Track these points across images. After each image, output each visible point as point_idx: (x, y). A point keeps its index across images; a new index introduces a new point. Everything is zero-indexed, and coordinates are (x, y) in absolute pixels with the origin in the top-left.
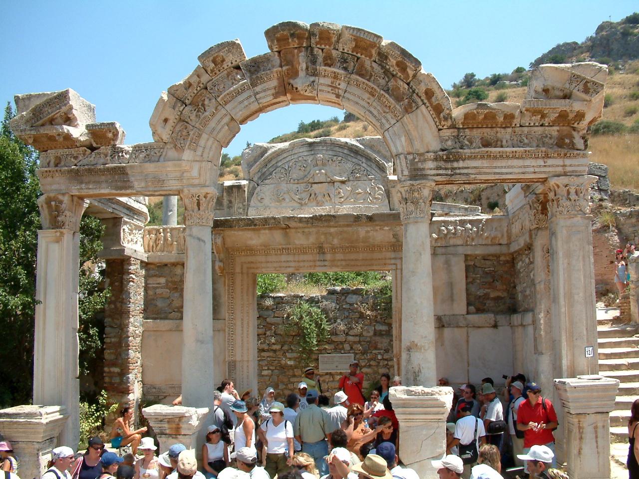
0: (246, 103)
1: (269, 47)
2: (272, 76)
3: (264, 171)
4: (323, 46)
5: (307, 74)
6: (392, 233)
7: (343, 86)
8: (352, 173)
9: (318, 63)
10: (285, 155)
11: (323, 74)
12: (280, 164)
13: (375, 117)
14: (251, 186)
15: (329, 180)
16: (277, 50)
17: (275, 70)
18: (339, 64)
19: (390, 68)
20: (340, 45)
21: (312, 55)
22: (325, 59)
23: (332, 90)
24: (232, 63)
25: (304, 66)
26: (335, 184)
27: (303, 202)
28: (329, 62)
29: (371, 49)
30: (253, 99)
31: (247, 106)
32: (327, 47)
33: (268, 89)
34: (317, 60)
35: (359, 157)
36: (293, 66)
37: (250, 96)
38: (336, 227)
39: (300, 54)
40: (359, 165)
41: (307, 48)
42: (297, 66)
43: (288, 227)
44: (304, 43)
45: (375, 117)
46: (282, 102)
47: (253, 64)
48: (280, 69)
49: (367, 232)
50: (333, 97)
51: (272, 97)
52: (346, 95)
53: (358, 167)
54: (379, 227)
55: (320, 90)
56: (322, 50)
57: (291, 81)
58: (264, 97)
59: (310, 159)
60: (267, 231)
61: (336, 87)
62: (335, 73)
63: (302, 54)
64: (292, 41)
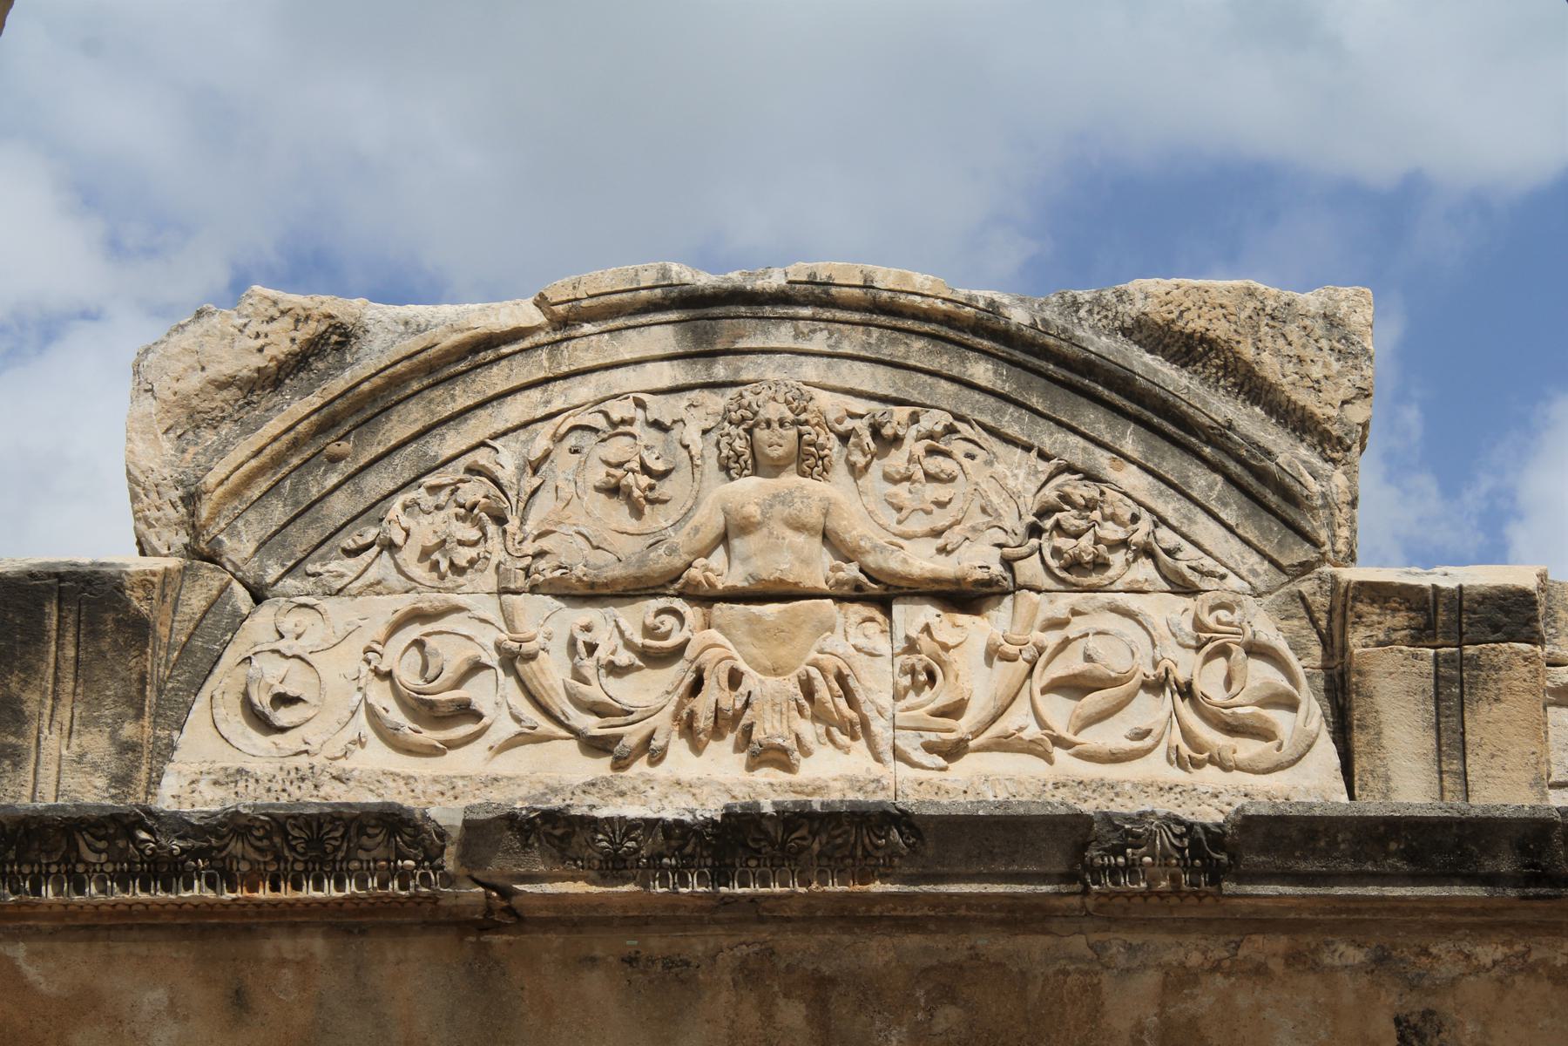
3: (315, 493)
6: (1390, 1001)
8: (1035, 531)
10: (497, 379)
12: (451, 442)
14: (195, 600)
15: (851, 571)
26: (898, 609)
27: (632, 736)
35: (1093, 419)
38: (915, 925)
40: (1091, 477)
43: (505, 914)
49: (1180, 980)
53: (1081, 491)
54: (1281, 943)
59: (697, 417)
60: (318, 945)
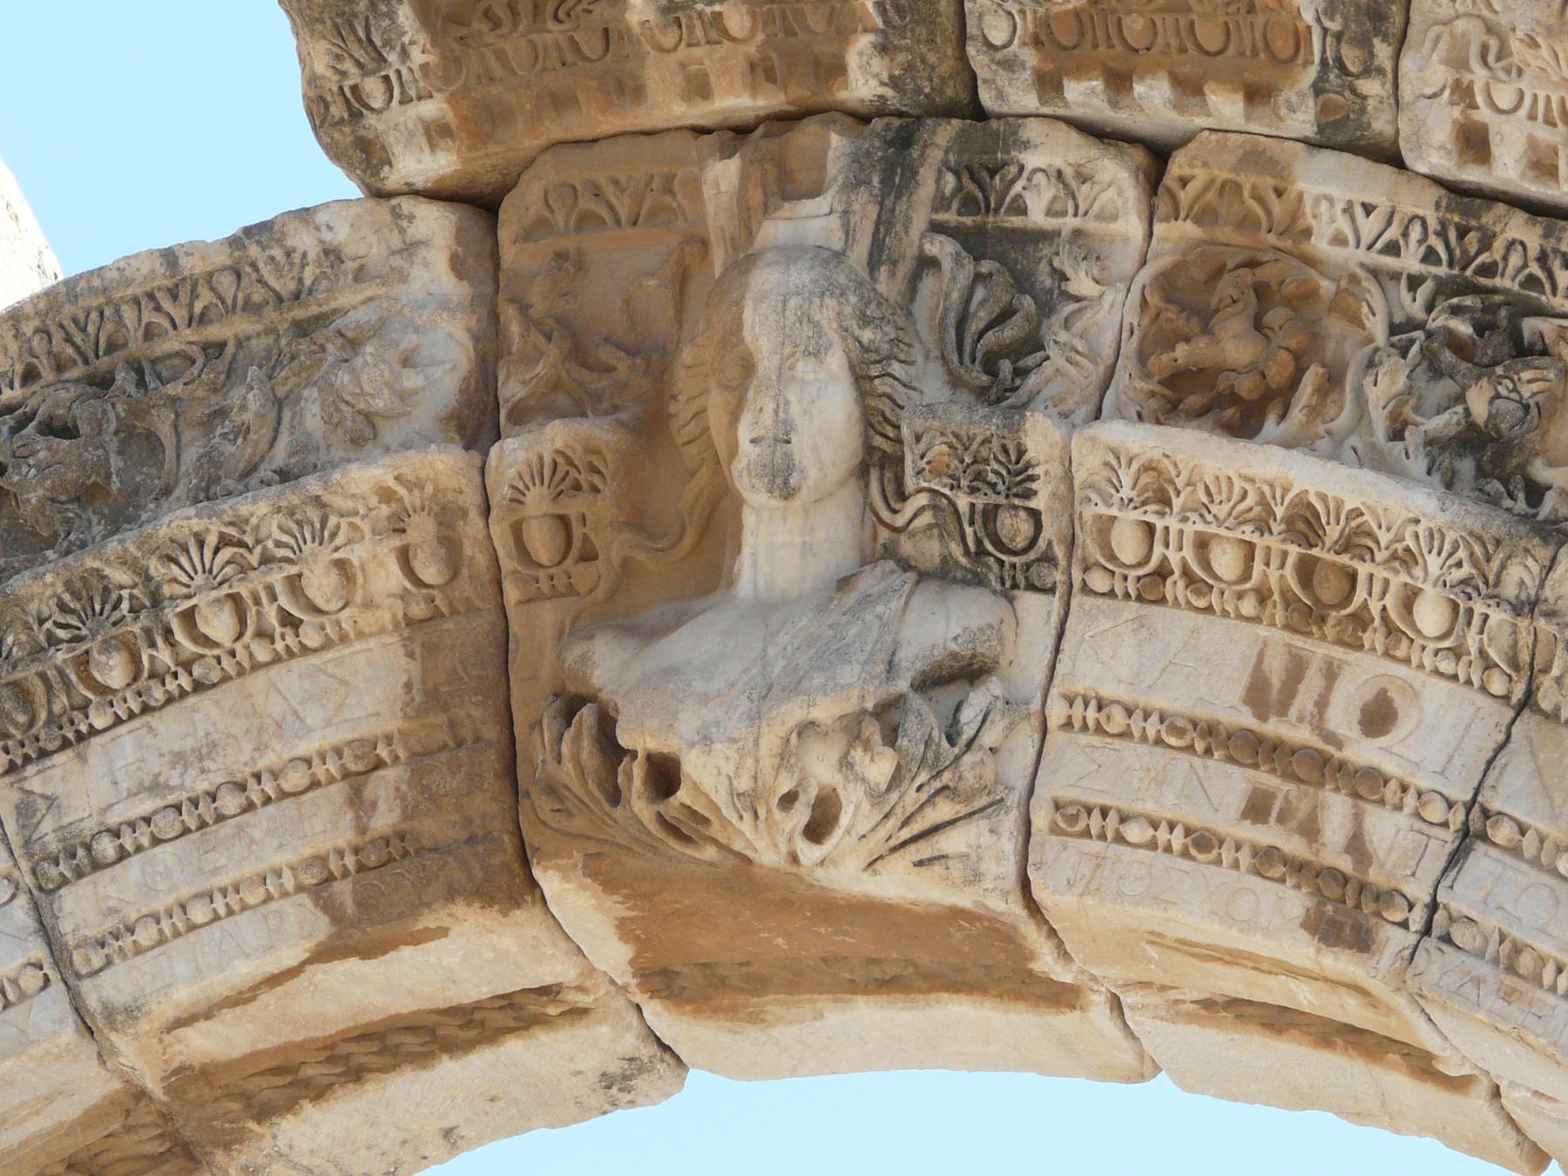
1: (318, 109)
2: (321, 584)
4: (1153, 104)
5: (882, 550)
9: (1061, 368)
11: (1128, 546)
17: (364, 477)
18: (1387, 384)
20: (1425, 70)
21: (974, 242)
22: (1183, 297)
25: (820, 413)
28: (1234, 347)
32: (1225, 107)
33: (255, 791)
34: (1055, 332)
36: (651, 425)
39: (775, 230)
41: (894, 136)
42: (716, 403)
46: (518, 1012)
47: (55, 397)
48: (445, 464)
50: (1273, 922)
51: (301, 926)
52: (1490, 890)
55: (1074, 817)
56: (1157, 155)
57: (607, 665)
58: (177, 923)
61: (1323, 767)
63: (814, 220)
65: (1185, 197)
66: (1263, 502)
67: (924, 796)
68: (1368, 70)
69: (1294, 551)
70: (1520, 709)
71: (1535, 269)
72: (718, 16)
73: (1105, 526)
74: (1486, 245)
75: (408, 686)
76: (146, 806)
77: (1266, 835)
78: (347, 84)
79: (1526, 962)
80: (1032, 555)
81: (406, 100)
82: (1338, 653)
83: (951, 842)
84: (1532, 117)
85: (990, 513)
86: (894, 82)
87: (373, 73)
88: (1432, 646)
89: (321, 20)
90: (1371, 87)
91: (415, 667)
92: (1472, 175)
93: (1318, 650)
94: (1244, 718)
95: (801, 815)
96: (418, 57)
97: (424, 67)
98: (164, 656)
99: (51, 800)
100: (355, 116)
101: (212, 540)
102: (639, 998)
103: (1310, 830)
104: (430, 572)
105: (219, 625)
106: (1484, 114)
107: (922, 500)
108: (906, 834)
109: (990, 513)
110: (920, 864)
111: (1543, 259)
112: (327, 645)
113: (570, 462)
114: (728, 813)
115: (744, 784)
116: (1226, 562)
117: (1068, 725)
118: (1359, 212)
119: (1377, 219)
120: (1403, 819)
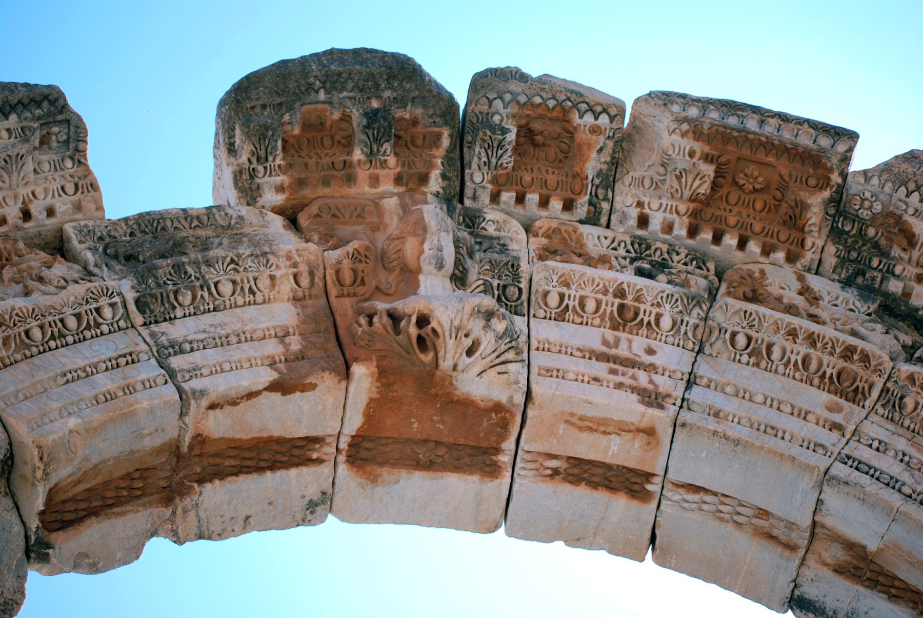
0: (105, 382)
2: (264, 283)
7: (672, 357)
13: (892, 483)
16: (279, 199)
19: (907, 294)
23: (613, 372)
24: (26, 215)
29: (803, 195)
30: (149, 369)
31: (110, 397)
32: (556, 205)
37: (132, 359)
44: (435, 174)
45: (892, 483)
55: (548, 372)
61: (631, 363)
62: (620, 293)
64: (371, 154)
65: (541, 232)
66: (605, 287)
67: (507, 347)
68: (605, 199)
69: (617, 301)
70: (698, 353)
71: (666, 256)
72: (385, 161)
73: (546, 294)
74: (648, 247)
75: (298, 314)
76: (202, 336)
77: (619, 379)
78: (252, 167)
79: (721, 414)
80: (519, 302)
81: (270, 175)
82: (630, 336)
83: (512, 367)
84: (665, 211)
85: (505, 287)
86: (443, 188)
87: (262, 164)
88: (665, 334)
89: (255, 135)
90: (605, 206)
91: (299, 310)
92: (640, 233)
93: (623, 336)
94: (604, 349)
95: (468, 342)
96: (278, 161)
97: (279, 166)
98: (206, 295)
99: (163, 334)
100: (252, 178)
101: (228, 260)
102: (342, 458)
103: (634, 377)
104: (305, 281)
105: (226, 288)
106: (647, 211)
107: (481, 282)
108: (497, 361)
109: (505, 287)
110: (499, 373)
111: (668, 253)
112: (264, 302)
113: (359, 253)
114: (447, 334)
115: (456, 323)
116: (591, 306)
117: (538, 349)
118: (602, 239)
119: (609, 241)
120: (666, 377)
